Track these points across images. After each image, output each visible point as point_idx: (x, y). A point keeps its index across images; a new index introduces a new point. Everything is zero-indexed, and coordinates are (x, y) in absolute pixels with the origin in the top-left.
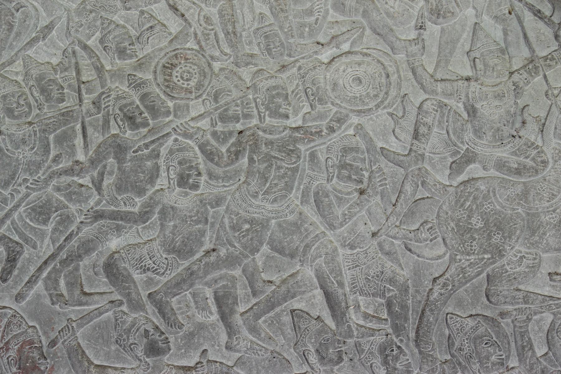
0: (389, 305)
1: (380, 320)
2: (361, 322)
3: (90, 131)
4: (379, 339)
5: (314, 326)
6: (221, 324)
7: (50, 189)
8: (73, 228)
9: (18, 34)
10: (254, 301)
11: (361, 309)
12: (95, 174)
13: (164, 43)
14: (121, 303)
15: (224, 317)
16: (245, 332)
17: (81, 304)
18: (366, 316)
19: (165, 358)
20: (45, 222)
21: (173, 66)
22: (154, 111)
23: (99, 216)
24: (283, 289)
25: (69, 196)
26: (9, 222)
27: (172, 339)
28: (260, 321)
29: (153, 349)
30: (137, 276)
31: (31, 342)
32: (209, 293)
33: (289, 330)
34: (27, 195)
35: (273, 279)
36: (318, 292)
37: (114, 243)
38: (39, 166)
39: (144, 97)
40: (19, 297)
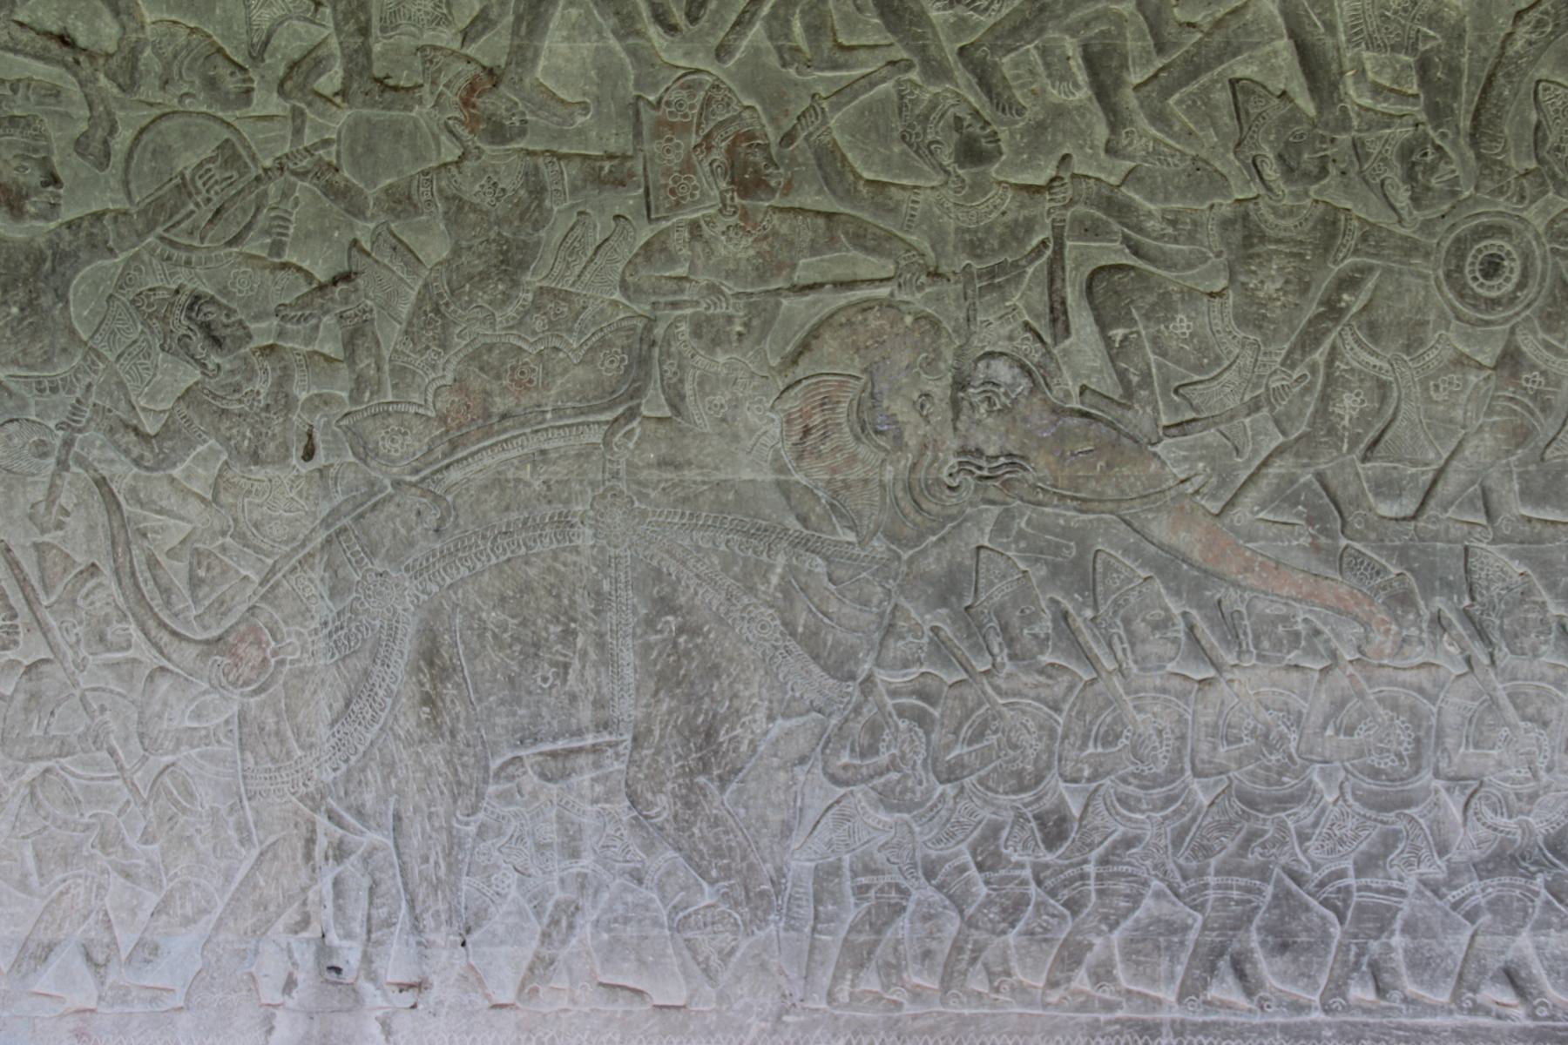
0: (1424, 67)
1: (1403, 96)
2: (1367, 102)
4: (1402, 132)
5: (1276, 110)
6: (1096, 106)
10: (1159, 63)
11: (1371, 79)
14: (909, 66)
15: (1104, 93)
16: (1142, 122)
17: (835, 66)
18: (1377, 90)
19: (993, 170)
24: (1218, 38)
27: (1004, 135)
28: (1171, 101)
29: (973, 153)
31: (750, 136)
32: (1071, 47)
33: (1227, 120)
35: (1197, 19)
36: (1284, 44)
40: (722, 52)
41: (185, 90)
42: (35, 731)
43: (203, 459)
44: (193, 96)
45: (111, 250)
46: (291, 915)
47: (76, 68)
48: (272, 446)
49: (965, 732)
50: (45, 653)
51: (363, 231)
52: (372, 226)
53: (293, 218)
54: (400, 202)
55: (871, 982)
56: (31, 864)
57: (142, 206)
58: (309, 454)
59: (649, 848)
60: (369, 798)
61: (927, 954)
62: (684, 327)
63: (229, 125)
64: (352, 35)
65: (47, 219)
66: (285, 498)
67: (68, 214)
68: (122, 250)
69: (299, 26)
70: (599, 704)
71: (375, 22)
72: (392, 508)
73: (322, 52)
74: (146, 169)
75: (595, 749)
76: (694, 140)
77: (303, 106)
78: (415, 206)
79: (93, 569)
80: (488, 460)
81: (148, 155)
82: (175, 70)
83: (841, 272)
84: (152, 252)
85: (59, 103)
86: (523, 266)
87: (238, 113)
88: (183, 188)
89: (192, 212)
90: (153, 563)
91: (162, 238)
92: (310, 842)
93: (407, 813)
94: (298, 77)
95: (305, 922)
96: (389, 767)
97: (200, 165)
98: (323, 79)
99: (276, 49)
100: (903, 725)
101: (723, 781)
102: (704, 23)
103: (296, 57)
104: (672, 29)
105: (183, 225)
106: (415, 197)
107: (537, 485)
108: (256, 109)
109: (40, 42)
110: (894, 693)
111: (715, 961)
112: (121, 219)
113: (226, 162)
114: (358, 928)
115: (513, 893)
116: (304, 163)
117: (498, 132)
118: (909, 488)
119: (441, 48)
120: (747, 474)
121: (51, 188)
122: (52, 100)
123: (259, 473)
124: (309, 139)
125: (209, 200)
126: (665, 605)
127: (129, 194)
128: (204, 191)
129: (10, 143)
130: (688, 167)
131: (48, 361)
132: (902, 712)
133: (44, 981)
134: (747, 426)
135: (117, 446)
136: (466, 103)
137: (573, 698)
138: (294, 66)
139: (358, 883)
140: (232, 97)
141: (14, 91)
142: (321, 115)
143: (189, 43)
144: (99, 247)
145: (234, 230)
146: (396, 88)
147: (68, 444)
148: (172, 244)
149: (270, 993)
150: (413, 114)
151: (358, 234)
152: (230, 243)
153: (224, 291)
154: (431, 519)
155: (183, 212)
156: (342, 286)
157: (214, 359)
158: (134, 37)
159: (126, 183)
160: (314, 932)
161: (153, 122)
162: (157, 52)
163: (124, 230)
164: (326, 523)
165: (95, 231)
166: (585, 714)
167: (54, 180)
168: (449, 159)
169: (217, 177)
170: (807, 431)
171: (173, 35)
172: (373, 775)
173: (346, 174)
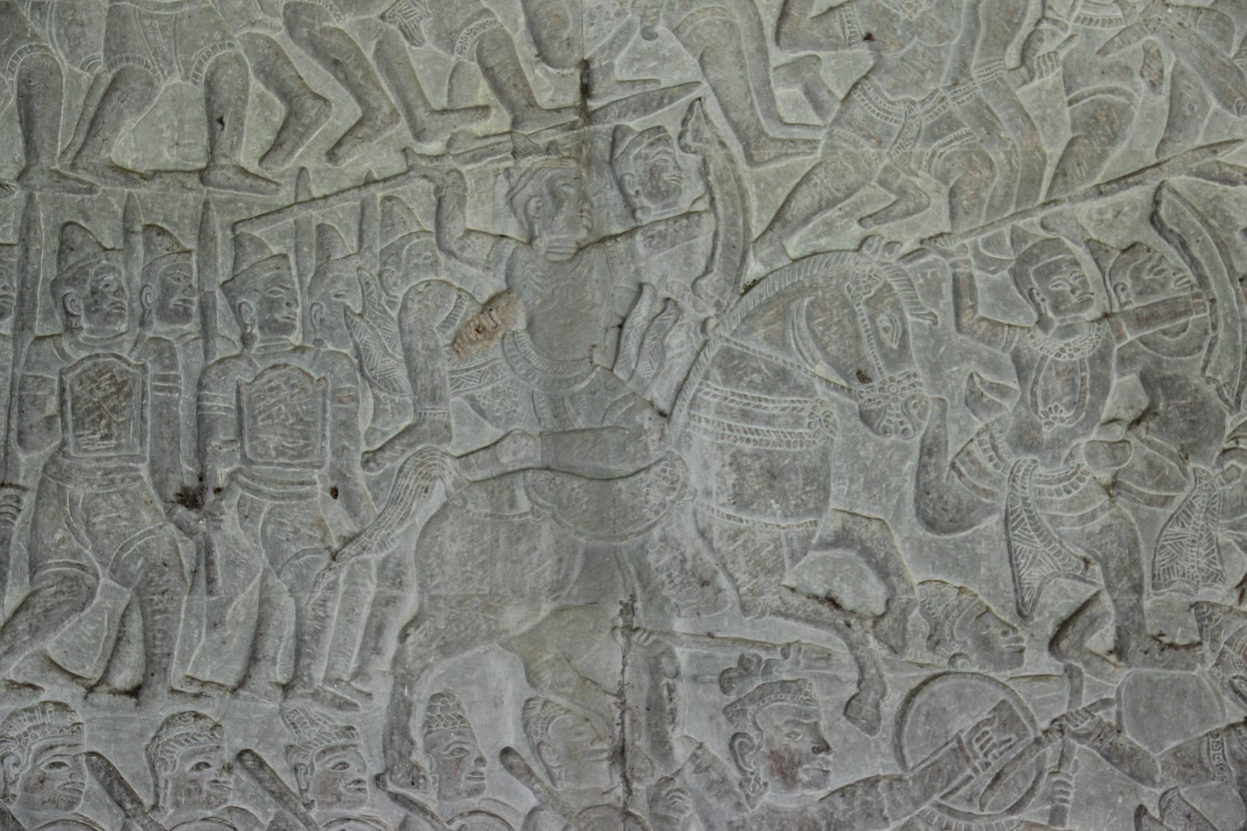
41: (957, 650)
44: (966, 656)
45: (886, 819)
47: (847, 630)
51: (1149, 797)
52: (1159, 791)
53: (1072, 783)
54: (1191, 766)
57: (917, 770)
63: (1005, 687)
64: (1127, 592)
65: (819, 787)
67: (836, 782)
68: (895, 819)
69: (1065, 583)
71: (1147, 580)
73: (1094, 610)
74: (920, 732)
77: (1080, 665)
78: (1207, 770)
81: (922, 718)
82: (946, 629)
84: (928, 822)
85: (829, 666)
87: (1009, 673)
89: (970, 778)
91: (939, 806)
97: (977, 727)
98: (1095, 637)
99: (1044, 607)
103: (1064, 614)
105: (961, 792)
106: (1206, 761)
108: (1028, 669)
109: (812, 606)
112: (896, 785)
113: (1004, 724)
116: (1085, 725)
119: (1218, 605)
121: (821, 755)
122: (823, 663)
124: (1086, 699)
125: (988, 764)
127: (902, 761)
128: (981, 755)
129: (781, 708)
138: (1064, 625)
140: (1006, 657)
141: (785, 656)
142: (1097, 674)
143: (960, 602)
145: (1015, 797)
146: (1171, 645)
148: (951, 812)
150: (1194, 673)
151: (1145, 801)
152: (1012, 810)
155: (961, 777)
158: (904, 598)
159: (898, 748)
161: (926, 683)
162: (926, 613)
163: (900, 798)
165: (869, 799)
168: (1234, 720)
169: (995, 740)
171: (943, 595)
173: (1129, 736)
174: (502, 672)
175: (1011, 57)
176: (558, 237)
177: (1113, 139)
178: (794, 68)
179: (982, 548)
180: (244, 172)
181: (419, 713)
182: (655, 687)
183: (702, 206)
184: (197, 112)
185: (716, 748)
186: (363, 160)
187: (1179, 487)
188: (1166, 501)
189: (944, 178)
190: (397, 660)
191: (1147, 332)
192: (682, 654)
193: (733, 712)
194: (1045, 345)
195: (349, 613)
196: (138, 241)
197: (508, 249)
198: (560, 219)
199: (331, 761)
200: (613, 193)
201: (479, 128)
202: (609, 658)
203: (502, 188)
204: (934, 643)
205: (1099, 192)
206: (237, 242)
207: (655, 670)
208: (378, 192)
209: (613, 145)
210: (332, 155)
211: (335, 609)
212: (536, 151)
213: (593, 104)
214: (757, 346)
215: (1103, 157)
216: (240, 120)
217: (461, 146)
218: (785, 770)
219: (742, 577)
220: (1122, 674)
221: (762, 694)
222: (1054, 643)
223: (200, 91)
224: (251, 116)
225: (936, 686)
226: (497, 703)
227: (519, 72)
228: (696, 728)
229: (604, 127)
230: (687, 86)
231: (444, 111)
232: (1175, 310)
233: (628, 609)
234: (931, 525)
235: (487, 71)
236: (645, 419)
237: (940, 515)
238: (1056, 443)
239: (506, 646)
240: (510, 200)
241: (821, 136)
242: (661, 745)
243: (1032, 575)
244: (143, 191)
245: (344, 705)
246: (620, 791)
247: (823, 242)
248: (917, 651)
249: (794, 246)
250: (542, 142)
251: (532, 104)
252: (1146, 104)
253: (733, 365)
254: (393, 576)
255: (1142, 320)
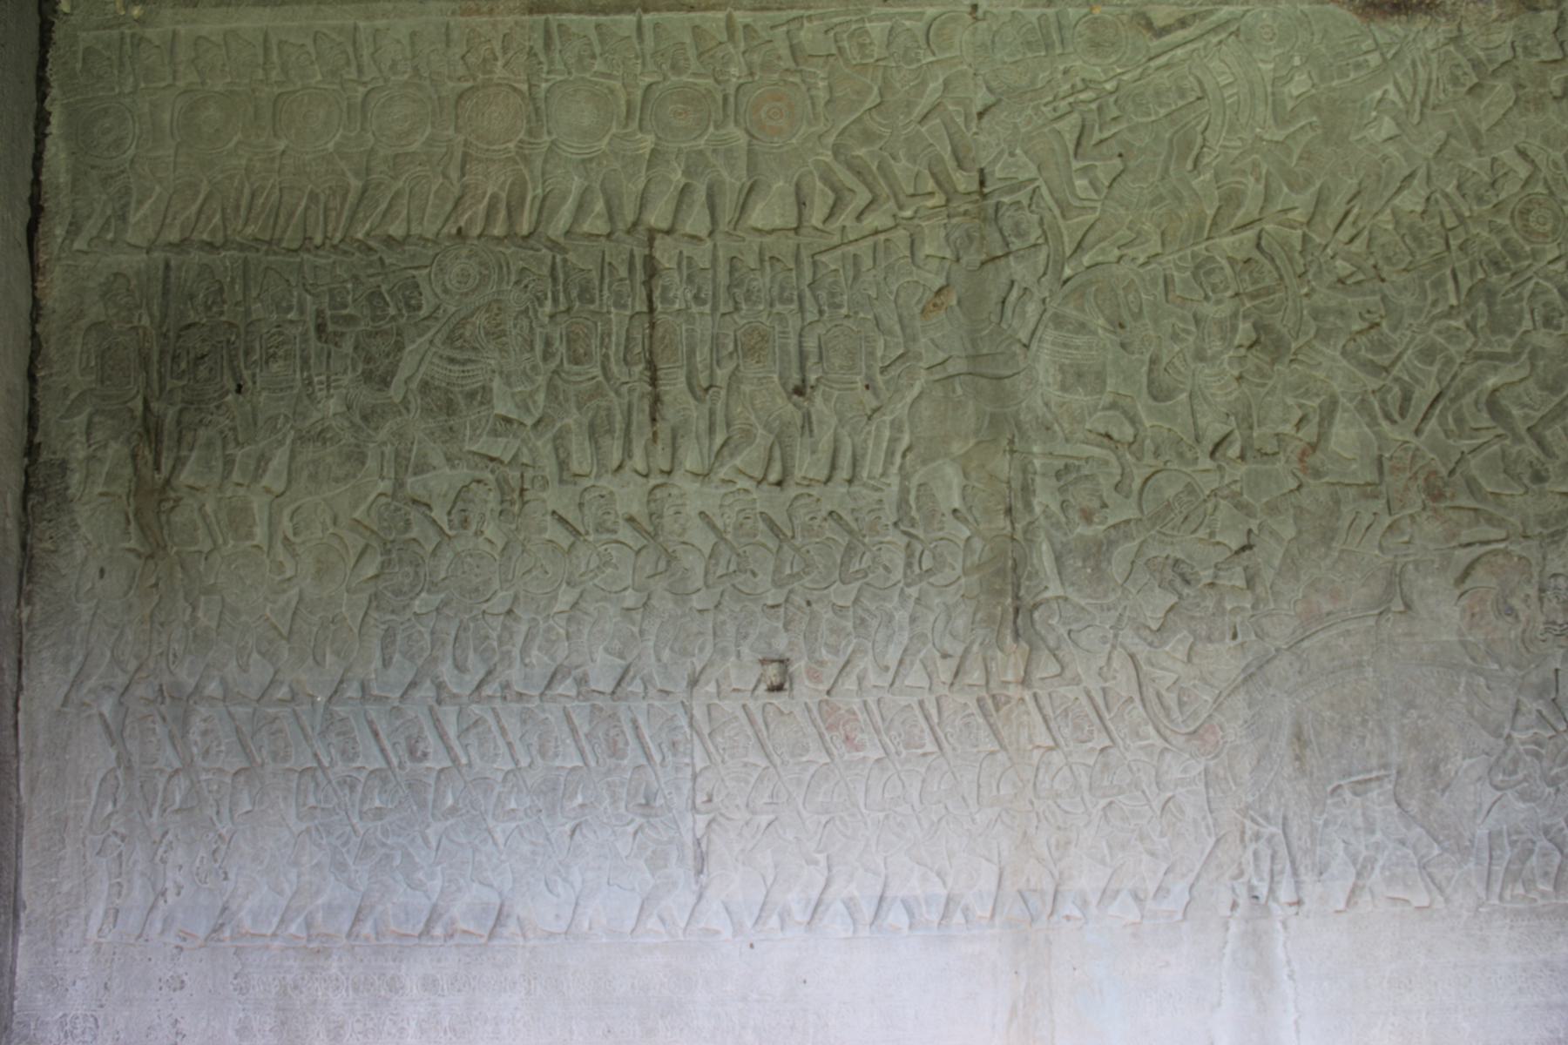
3: (1460, 276)
7: (1431, 332)
8: (1456, 368)
9: (1387, 185)
12: (1468, 317)
13: (1517, 188)
17: (1472, 438)
19: (1547, 486)
20: (1431, 363)
21: (1529, 211)
22: (1516, 256)
23: (1478, 357)
25: (1449, 339)
26: (1399, 364)
30: (1516, 412)
34: (1413, 339)
37: (1491, 381)
38: (1421, 310)
39: (1505, 243)
40: (1417, 432)
42: (1106, 783)
43: (1181, 641)
46: (1234, 870)
48: (1217, 634)
49: (1558, 761)
50: (1107, 743)
55: (1520, 890)
56: (1106, 851)
58: (1235, 636)
59: (1408, 827)
60: (1271, 809)
61: (1546, 874)
62: (1411, 567)
66: (1225, 661)
67: (1111, 522)
69: (1218, 425)
70: (1382, 755)
72: (1277, 662)
75: (1378, 778)
76: (1408, 474)
79: (1131, 699)
80: (1322, 636)
83: (1483, 537)
86: (1332, 539)
88: (1169, 506)
90: (1159, 696)
92: (1243, 833)
93: (1290, 815)
94: (1221, 449)
95: (1241, 874)
96: (1280, 793)
100: (1528, 759)
101: (1443, 791)
102: (1408, 418)
104: (1394, 422)
107: (1346, 647)
109: (1100, 438)
110: (1523, 743)
111: (1444, 883)
114: (1266, 876)
115: (1341, 853)
117: (1317, 474)
118: (1523, 641)
120: (1445, 638)
123: (1210, 647)
124: (1227, 480)
126: (1410, 705)
127: (1142, 511)
130: (1407, 489)
131: (1106, 595)
132: (1527, 752)
133: (1113, 909)
134: (1443, 614)
135: (1140, 637)
136: (1301, 460)
137: (1368, 754)
138: (1217, 446)
139: (1266, 853)
144: (1128, 537)
147: (1116, 636)
149: (1225, 911)
153: (1190, 557)
154: (1297, 665)
156: (1248, 552)
157: (1186, 591)
160: (1244, 879)
164: (1244, 670)
166: (1374, 761)
167: (1104, 506)
170: (1473, 615)
172: (1273, 797)
174: (951, 473)
175: (1189, 165)
176: (972, 257)
177: (1239, 206)
178: (1085, 171)
179: (1179, 409)
180: (816, 228)
181: (913, 493)
182: (1025, 479)
183: (1041, 241)
184: (792, 199)
185: (1055, 507)
186: (872, 221)
187: (1270, 378)
188: (1264, 385)
189: (1158, 226)
190: (901, 468)
191: (1256, 302)
192: (1037, 463)
193: (1062, 490)
194: (1208, 309)
195: (877, 445)
196: (767, 264)
197: (947, 264)
198: (972, 250)
199: (873, 516)
200: (997, 235)
201: (930, 203)
202: (1003, 465)
203: (943, 234)
204: (1157, 454)
205: (1233, 232)
206: (815, 264)
207: (1024, 471)
208: (882, 237)
209: (997, 211)
210: (859, 218)
211: (871, 443)
212: (958, 215)
213: (986, 190)
214: (1070, 311)
215: (1234, 215)
216: (812, 202)
217: (922, 213)
218: (1087, 516)
219: (1066, 425)
220: (1243, 468)
221: (1076, 481)
222: (1212, 454)
223: (792, 189)
224: (817, 200)
225: (1158, 476)
226: (949, 487)
227: (949, 175)
228: (1044, 498)
229: (992, 202)
230: (1032, 180)
231: (913, 196)
232: (1269, 291)
233: (1011, 442)
234: (1155, 398)
235: (933, 175)
236: (1017, 348)
237: (1159, 393)
238: (1214, 357)
239: (954, 460)
240: (947, 237)
241: (1098, 205)
242: (1028, 506)
243: (1202, 422)
244: (768, 239)
245: (877, 490)
246: (1009, 528)
247: (1100, 259)
248: (1149, 459)
249: (1086, 260)
250: (962, 209)
251: (956, 191)
252: (1252, 187)
253: (1059, 321)
254: (897, 426)
255: (1253, 297)
